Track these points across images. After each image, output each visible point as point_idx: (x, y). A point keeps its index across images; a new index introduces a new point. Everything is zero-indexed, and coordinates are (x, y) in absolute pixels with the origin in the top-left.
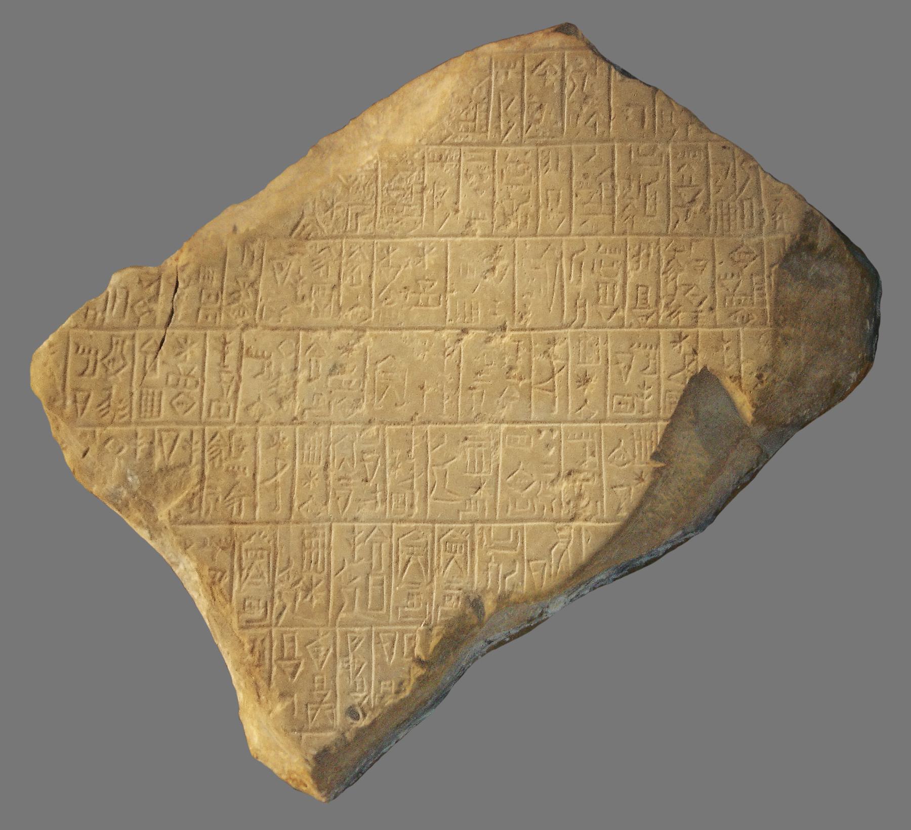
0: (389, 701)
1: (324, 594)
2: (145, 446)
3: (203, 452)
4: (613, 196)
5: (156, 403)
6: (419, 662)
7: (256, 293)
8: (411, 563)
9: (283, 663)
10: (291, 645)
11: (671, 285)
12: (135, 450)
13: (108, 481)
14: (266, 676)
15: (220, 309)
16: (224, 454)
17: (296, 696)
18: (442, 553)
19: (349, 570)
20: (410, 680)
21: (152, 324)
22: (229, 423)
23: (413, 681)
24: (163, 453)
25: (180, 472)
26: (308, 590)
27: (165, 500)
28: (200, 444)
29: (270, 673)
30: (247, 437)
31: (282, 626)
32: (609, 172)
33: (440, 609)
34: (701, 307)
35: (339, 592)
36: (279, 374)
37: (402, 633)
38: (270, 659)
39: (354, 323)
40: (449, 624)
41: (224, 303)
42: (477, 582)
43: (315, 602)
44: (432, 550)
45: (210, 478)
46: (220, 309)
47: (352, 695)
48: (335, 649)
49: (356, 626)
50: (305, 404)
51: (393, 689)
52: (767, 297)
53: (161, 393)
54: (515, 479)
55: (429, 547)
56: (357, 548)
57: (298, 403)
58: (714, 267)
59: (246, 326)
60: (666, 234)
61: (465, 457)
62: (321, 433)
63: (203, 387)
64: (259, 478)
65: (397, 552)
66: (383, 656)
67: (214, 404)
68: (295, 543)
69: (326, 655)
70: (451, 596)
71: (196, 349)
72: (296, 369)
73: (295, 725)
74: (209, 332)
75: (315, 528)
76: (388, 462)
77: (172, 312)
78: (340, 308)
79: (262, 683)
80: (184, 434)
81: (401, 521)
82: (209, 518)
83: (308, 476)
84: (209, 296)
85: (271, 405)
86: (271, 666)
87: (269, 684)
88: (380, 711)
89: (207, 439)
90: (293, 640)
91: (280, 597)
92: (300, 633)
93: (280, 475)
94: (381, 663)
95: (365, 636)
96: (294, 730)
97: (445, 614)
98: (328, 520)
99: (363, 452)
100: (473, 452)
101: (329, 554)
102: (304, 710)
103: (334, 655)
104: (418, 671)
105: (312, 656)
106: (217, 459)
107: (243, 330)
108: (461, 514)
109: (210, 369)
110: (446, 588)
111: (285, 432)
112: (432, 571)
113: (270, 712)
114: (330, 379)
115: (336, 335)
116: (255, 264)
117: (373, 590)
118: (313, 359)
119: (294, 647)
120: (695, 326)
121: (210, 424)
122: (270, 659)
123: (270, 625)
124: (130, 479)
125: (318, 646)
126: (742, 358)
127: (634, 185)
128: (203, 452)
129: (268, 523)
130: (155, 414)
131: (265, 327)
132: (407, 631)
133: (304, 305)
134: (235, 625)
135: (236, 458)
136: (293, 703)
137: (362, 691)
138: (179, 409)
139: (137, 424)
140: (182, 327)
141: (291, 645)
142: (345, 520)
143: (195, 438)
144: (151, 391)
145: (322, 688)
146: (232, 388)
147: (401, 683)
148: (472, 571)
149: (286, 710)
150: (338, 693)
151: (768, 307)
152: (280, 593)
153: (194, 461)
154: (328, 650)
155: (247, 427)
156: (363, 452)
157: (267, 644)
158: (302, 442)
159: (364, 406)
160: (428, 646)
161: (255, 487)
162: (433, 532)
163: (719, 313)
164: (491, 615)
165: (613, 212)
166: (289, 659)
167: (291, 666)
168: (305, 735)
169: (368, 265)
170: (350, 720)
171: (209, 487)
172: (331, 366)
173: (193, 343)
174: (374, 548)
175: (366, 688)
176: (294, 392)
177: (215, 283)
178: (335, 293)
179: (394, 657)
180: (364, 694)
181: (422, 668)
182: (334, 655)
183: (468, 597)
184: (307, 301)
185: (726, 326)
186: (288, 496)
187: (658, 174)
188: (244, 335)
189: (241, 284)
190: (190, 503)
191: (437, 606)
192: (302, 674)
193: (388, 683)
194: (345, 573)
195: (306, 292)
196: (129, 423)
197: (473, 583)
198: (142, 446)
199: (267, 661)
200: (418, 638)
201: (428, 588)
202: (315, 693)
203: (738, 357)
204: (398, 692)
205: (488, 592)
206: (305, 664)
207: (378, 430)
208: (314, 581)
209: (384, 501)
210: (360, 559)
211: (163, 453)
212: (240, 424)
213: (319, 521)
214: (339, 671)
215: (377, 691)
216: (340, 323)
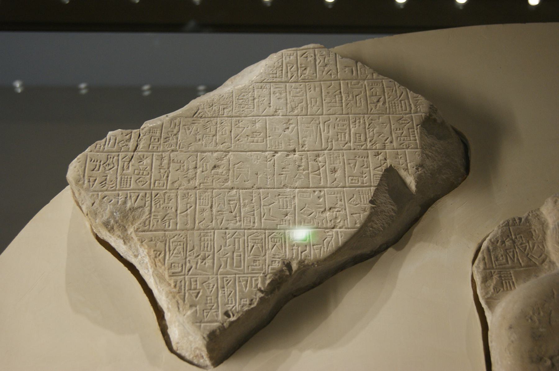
0: (246, 309)
1: (212, 261)
2: (123, 199)
3: (151, 201)
4: (342, 100)
5: (128, 182)
6: (260, 290)
7: (177, 138)
8: (255, 247)
9: (191, 291)
10: (195, 283)
11: (371, 133)
12: (118, 201)
13: (104, 216)
14: (182, 297)
15: (160, 144)
16: (161, 202)
17: (198, 306)
18: (270, 242)
19: (224, 250)
20: (256, 299)
21: (128, 151)
22: (164, 190)
23: (258, 299)
24: (131, 202)
25: (140, 210)
26: (204, 259)
27: (132, 224)
28: (149, 199)
29: (185, 296)
30: (173, 195)
31: (191, 275)
32: (339, 91)
33: (270, 267)
34: (387, 142)
35: (219, 259)
36: (188, 170)
37: (252, 277)
38: (185, 290)
39: (224, 149)
40: (275, 274)
41: (162, 142)
42: (288, 255)
43: (207, 265)
44: (265, 242)
45: (154, 212)
46: (160, 144)
47: (227, 306)
48: (217, 285)
49: (229, 274)
50: (201, 181)
51: (248, 303)
52: (417, 138)
53: (131, 178)
54: (304, 211)
55: (263, 240)
56: (228, 241)
57: (197, 181)
58: (391, 126)
59: (173, 151)
60: (367, 114)
61: (279, 202)
62: (209, 193)
63: (151, 175)
64: (179, 212)
65: (248, 242)
66: (242, 287)
67: (157, 182)
68: (196, 239)
69: (213, 288)
70: (275, 261)
71: (148, 161)
72: (196, 168)
73: (197, 321)
74: (154, 153)
75: (207, 233)
76: (242, 204)
77: (137, 146)
78: (217, 144)
79: (181, 302)
80: (142, 194)
81: (249, 229)
82: (154, 229)
83: (203, 210)
84: (155, 139)
85: (185, 183)
86: (185, 293)
87: (184, 301)
88: (241, 313)
89: (153, 196)
90: (196, 281)
91: (189, 262)
92: (199, 278)
93: (189, 211)
94: (241, 291)
95: (233, 279)
96: (197, 322)
97: (272, 269)
98: (213, 229)
99: (230, 201)
100: (283, 201)
101: (214, 243)
102: (202, 313)
103: (217, 287)
104: (260, 295)
105: (206, 288)
106: (158, 204)
107: (171, 152)
108: (278, 226)
109: (155, 168)
110: (273, 258)
111: (192, 192)
112: (265, 251)
113: (184, 315)
114: (213, 171)
115: (215, 154)
116: (176, 127)
117: (236, 259)
118: (204, 163)
119: (197, 284)
120: (384, 149)
121: (155, 190)
122: (185, 290)
123: (185, 275)
124: (115, 214)
125: (209, 283)
126: (408, 161)
127: (351, 97)
128: (151, 201)
129: (183, 230)
130: (128, 186)
131: (181, 151)
132: (254, 277)
133: (200, 143)
134: (167, 276)
135: (168, 203)
136: (196, 310)
137: (232, 304)
138: (139, 184)
139: (119, 190)
140: (142, 151)
141: (195, 283)
142: (221, 229)
143: (147, 196)
144: (126, 177)
145: (211, 303)
146: (166, 175)
147: (252, 300)
148: (285, 251)
149: (193, 313)
150: (220, 305)
151: (418, 141)
152: (189, 261)
153: (147, 205)
154: (214, 285)
155: (173, 191)
156: (230, 201)
157: (183, 283)
158: (200, 196)
159: (229, 182)
160: (265, 283)
161: (177, 215)
162: (265, 233)
163: (395, 144)
164: (296, 271)
165: (342, 106)
166: (195, 289)
167: (195, 293)
168: (203, 325)
169: (230, 127)
170: (226, 318)
171: (154, 216)
172: (213, 166)
173: (147, 158)
174: (236, 242)
175: (234, 302)
176: (196, 176)
177: (158, 134)
178: (214, 138)
179: (248, 288)
180: (233, 305)
181: (262, 293)
182: (217, 287)
183: (284, 262)
184: (201, 141)
185: (399, 149)
186: (193, 219)
187: (361, 92)
188: (171, 155)
189: (170, 135)
190: (145, 223)
191: (269, 266)
192: (200, 297)
193: (245, 300)
194: (222, 252)
195: (201, 138)
196: (115, 190)
197: (286, 256)
198: (121, 200)
199: (183, 291)
200: (260, 279)
201: (264, 258)
202: (208, 305)
203: (406, 161)
204: (250, 304)
205: (294, 260)
206: (203, 292)
207: (236, 192)
208: (207, 256)
209: (240, 221)
210: (229, 246)
211: (131, 202)
212: (170, 190)
213: (208, 229)
214: (220, 295)
215: (240, 304)
216: (217, 149)
